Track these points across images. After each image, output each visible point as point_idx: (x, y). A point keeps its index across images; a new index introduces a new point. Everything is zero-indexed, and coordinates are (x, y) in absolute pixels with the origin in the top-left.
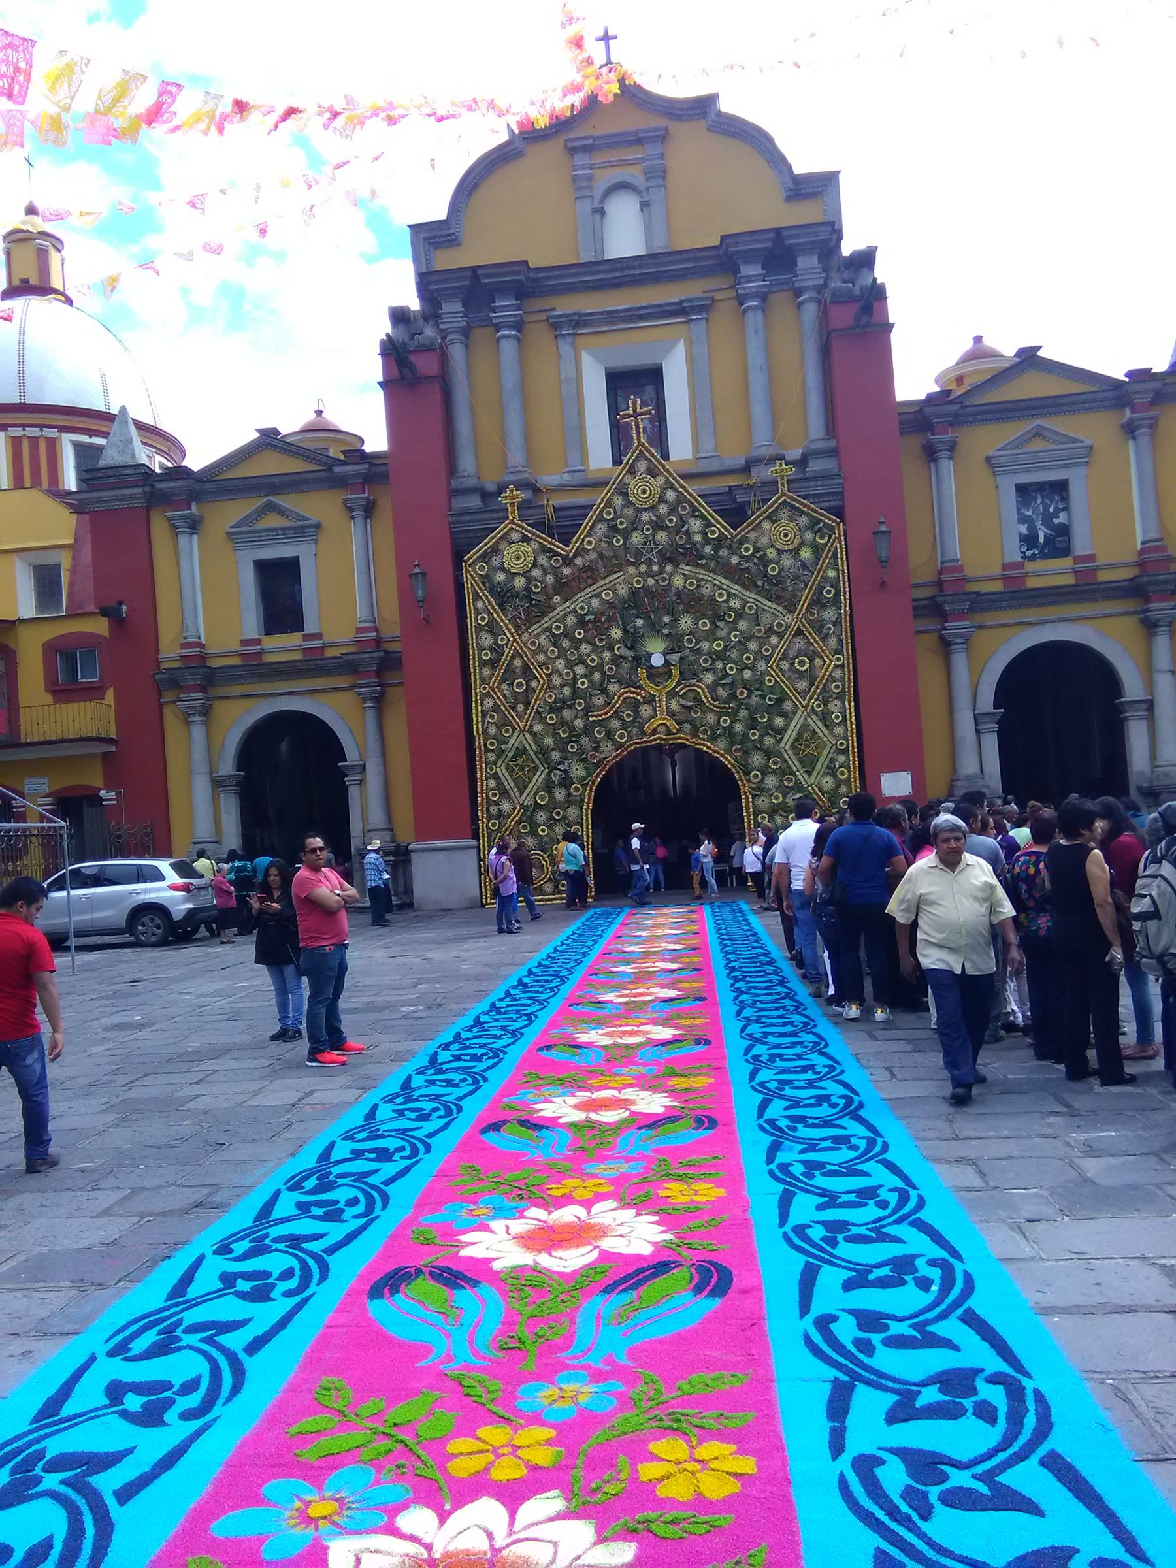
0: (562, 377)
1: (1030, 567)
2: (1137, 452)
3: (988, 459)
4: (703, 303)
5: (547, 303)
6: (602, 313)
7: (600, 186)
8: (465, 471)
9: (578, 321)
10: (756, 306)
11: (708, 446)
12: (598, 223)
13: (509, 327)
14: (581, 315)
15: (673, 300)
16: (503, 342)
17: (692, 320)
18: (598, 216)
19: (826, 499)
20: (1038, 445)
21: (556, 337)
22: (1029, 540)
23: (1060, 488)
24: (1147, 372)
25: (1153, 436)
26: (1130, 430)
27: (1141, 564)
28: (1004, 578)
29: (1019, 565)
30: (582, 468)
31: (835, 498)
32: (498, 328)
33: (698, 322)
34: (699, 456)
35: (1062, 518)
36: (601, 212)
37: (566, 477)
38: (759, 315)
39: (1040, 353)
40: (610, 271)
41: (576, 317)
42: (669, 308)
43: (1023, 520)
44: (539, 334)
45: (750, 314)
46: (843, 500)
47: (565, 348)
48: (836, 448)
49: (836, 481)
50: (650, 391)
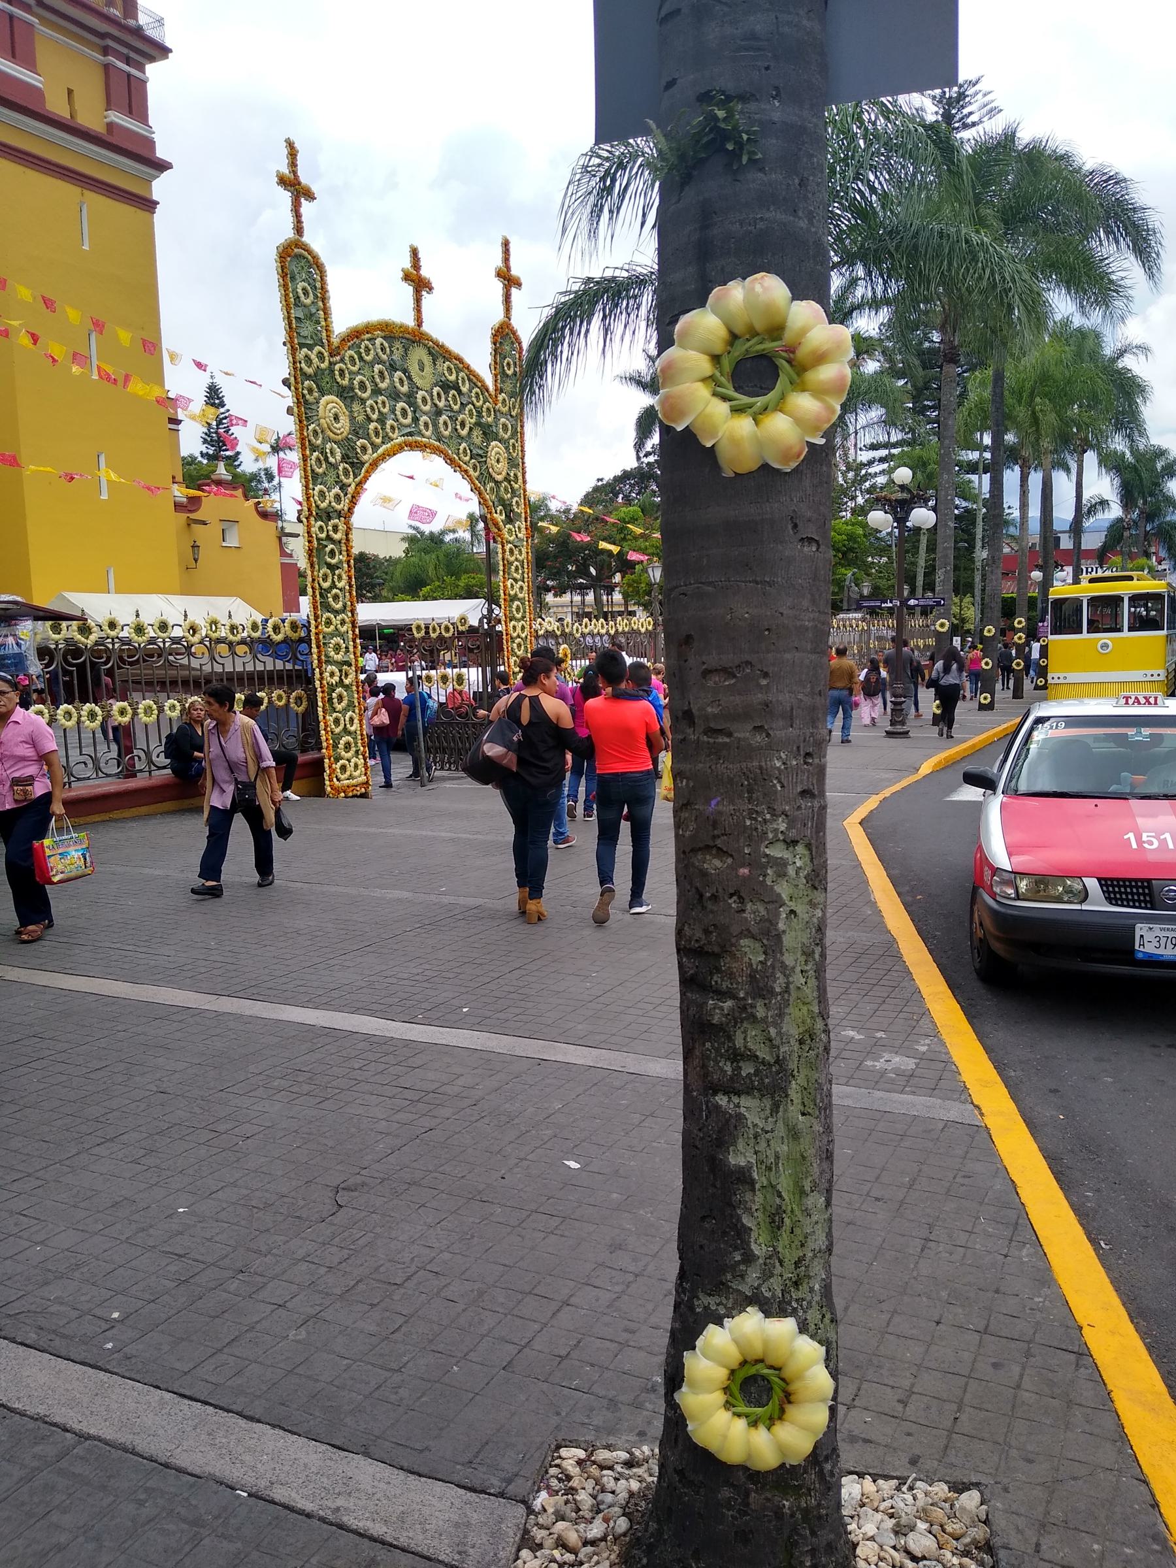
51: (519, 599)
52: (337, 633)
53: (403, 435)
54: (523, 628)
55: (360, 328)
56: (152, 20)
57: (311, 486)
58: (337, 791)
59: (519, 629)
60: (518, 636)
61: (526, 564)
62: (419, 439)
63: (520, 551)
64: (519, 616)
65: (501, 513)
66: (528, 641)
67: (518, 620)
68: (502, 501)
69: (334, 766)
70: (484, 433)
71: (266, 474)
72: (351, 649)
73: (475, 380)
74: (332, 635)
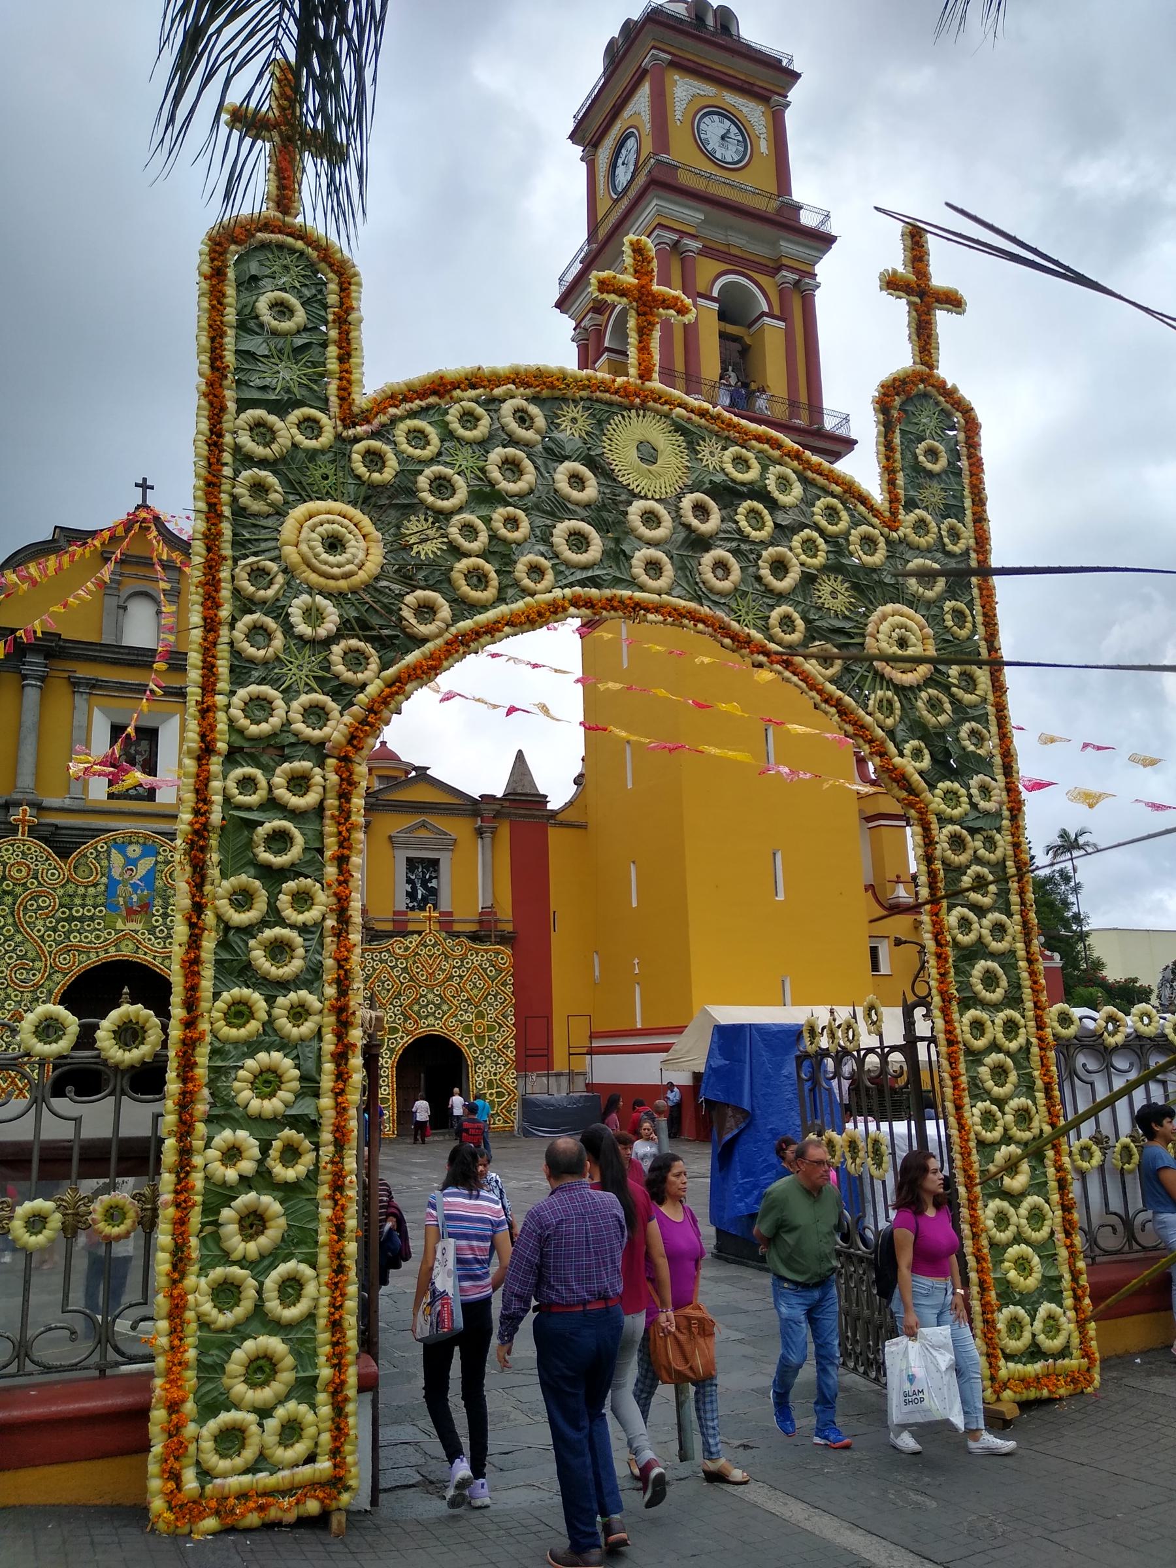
1: (411, 915)
2: (483, 847)
3: (390, 837)
5: (70, 665)
7: (126, 591)
9: (94, 685)
12: (120, 618)
13: (36, 679)
14: (97, 680)
16: (28, 689)
18: (121, 611)
20: (423, 833)
22: (411, 895)
23: (435, 863)
24: (493, 797)
25: (493, 839)
26: (480, 832)
27: (481, 922)
28: (394, 921)
29: (404, 913)
32: (25, 677)
35: (434, 884)
36: (125, 608)
39: (428, 772)
40: (128, 654)
43: (409, 881)
44: (60, 688)
47: (80, 701)
51: (992, 956)
52: (270, 1038)
53: (562, 588)
54: (1011, 1028)
55: (449, 377)
56: (838, 420)
57: (223, 685)
58: (189, 1510)
59: (995, 1031)
60: (995, 1047)
61: (1012, 870)
62: (626, 593)
63: (990, 844)
64: (997, 995)
65: (917, 754)
66: (1035, 1060)
67: (996, 1007)
68: (919, 729)
69: (191, 1429)
70: (856, 587)
71: (1061, 875)
72: (327, 1082)
73: (820, 480)
74: (252, 1047)
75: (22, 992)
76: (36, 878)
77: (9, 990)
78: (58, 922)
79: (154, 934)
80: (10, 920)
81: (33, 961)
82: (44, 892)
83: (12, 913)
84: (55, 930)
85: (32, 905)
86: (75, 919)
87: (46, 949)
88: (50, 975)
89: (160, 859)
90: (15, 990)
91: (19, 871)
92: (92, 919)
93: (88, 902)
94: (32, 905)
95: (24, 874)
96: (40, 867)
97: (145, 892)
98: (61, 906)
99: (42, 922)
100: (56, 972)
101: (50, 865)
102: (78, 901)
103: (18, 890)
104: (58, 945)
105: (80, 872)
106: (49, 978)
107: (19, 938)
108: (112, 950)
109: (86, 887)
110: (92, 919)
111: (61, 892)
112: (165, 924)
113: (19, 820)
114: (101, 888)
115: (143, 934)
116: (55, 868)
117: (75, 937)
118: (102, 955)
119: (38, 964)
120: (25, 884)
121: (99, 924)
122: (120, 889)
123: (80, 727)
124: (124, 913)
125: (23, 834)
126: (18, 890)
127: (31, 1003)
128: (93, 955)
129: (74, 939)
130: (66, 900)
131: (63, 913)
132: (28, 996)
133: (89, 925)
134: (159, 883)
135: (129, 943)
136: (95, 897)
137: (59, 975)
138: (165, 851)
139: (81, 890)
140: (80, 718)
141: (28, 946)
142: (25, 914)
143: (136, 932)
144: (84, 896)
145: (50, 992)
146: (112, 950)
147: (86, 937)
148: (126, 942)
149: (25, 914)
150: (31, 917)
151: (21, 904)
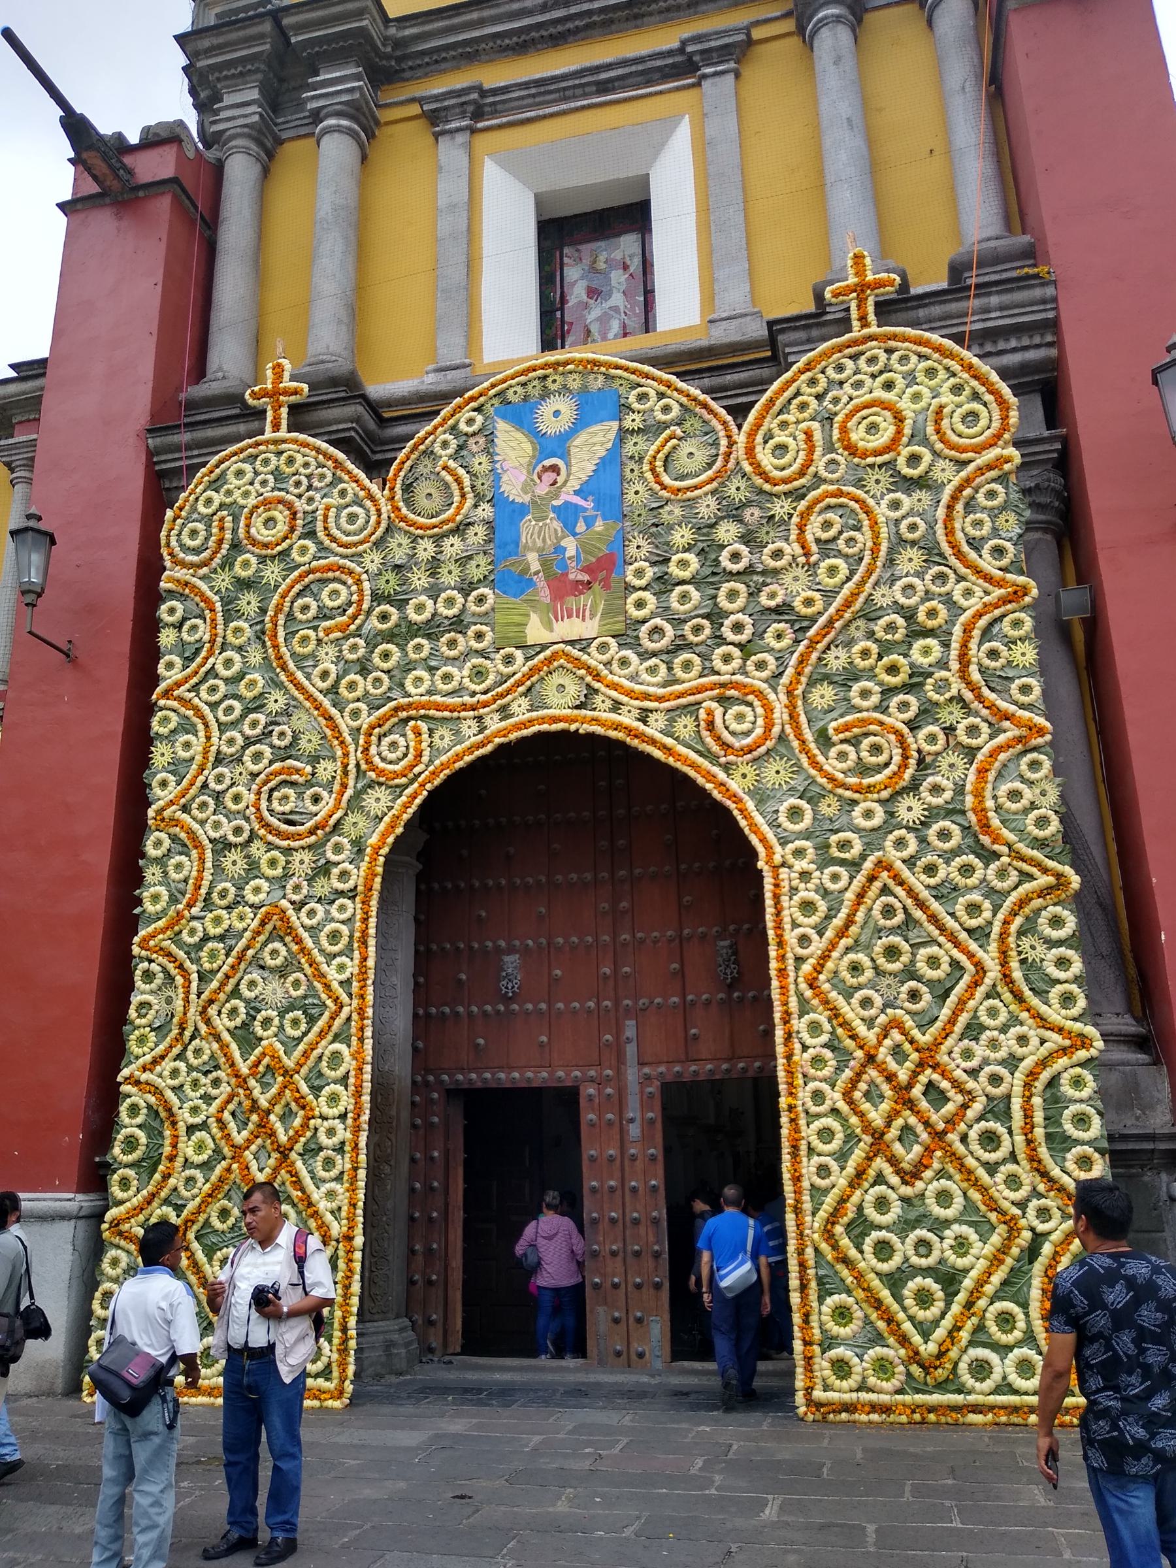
0: (442, 202)
4: (727, 40)
6: (525, 85)
8: (220, 369)
10: (838, 16)
11: (735, 297)
13: (339, 114)
14: (483, 93)
15: (665, 47)
16: (325, 141)
17: (705, 76)
19: (1013, 343)
21: (437, 136)
30: (467, 361)
31: (1037, 340)
33: (717, 79)
34: (715, 316)
37: (431, 378)
38: (844, 34)
41: (474, 96)
42: (659, 63)
45: (825, 33)
46: (1058, 343)
47: (451, 152)
48: (1032, 245)
49: (1037, 293)
50: (628, 244)
75: (287, 851)
76: (311, 534)
77: (257, 849)
78: (371, 646)
79: (635, 644)
80: (255, 657)
81: (314, 760)
82: (329, 569)
83: (260, 636)
84: (364, 669)
85: (306, 608)
86: (414, 630)
87: (344, 723)
88: (358, 795)
89: (632, 421)
90: (270, 846)
91: (270, 522)
92: (458, 624)
93: (449, 577)
94: (306, 608)
95: (282, 528)
96: (320, 504)
97: (599, 526)
98: (377, 597)
99: (332, 651)
100: (370, 785)
101: (343, 493)
102: (419, 579)
103: (272, 572)
104: (373, 708)
105: (422, 502)
106: (355, 805)
107: (276, 701)
108: (520, 708)
109: (438, 539)
110: (458, 624)
111: (373, 561)
112: (664, 611)
113: (265, 394)
114: (476, 536)
115: (603, 647)
116: (358, 502)
117: (418, 680)
118: (494, 724)
119: (326, 769)
120: (285, 553)
121: (479, 636)
122: (528, 529)
123: (452, 207)
124: (545, 595)
125: (276, 427)
126: (272, 572)
127: (310, 880)
128: (469, 728)
129: (417, 686)
130: (390, 583)
131: (384, 617)
132: (303, 862)
133: (452, 644)
134: (637, 494)
135: (567, 681)
136: (463, 561)
137: (382, 793)
138: (643, 397)
139: (426, 549)
140: (451, 188)
141: (300, 720)
142: (290, 635)
143: (582, 644)
144: (434, 567)
145: (359, 846)
146: (520, 708)
147: (447, 677)
148: (556, 679)
149: (290, 635)
150: (305, 640)
151: (279, 609)
